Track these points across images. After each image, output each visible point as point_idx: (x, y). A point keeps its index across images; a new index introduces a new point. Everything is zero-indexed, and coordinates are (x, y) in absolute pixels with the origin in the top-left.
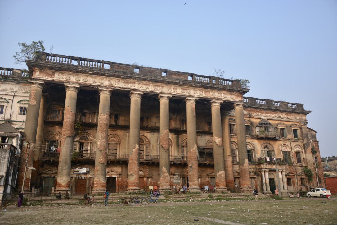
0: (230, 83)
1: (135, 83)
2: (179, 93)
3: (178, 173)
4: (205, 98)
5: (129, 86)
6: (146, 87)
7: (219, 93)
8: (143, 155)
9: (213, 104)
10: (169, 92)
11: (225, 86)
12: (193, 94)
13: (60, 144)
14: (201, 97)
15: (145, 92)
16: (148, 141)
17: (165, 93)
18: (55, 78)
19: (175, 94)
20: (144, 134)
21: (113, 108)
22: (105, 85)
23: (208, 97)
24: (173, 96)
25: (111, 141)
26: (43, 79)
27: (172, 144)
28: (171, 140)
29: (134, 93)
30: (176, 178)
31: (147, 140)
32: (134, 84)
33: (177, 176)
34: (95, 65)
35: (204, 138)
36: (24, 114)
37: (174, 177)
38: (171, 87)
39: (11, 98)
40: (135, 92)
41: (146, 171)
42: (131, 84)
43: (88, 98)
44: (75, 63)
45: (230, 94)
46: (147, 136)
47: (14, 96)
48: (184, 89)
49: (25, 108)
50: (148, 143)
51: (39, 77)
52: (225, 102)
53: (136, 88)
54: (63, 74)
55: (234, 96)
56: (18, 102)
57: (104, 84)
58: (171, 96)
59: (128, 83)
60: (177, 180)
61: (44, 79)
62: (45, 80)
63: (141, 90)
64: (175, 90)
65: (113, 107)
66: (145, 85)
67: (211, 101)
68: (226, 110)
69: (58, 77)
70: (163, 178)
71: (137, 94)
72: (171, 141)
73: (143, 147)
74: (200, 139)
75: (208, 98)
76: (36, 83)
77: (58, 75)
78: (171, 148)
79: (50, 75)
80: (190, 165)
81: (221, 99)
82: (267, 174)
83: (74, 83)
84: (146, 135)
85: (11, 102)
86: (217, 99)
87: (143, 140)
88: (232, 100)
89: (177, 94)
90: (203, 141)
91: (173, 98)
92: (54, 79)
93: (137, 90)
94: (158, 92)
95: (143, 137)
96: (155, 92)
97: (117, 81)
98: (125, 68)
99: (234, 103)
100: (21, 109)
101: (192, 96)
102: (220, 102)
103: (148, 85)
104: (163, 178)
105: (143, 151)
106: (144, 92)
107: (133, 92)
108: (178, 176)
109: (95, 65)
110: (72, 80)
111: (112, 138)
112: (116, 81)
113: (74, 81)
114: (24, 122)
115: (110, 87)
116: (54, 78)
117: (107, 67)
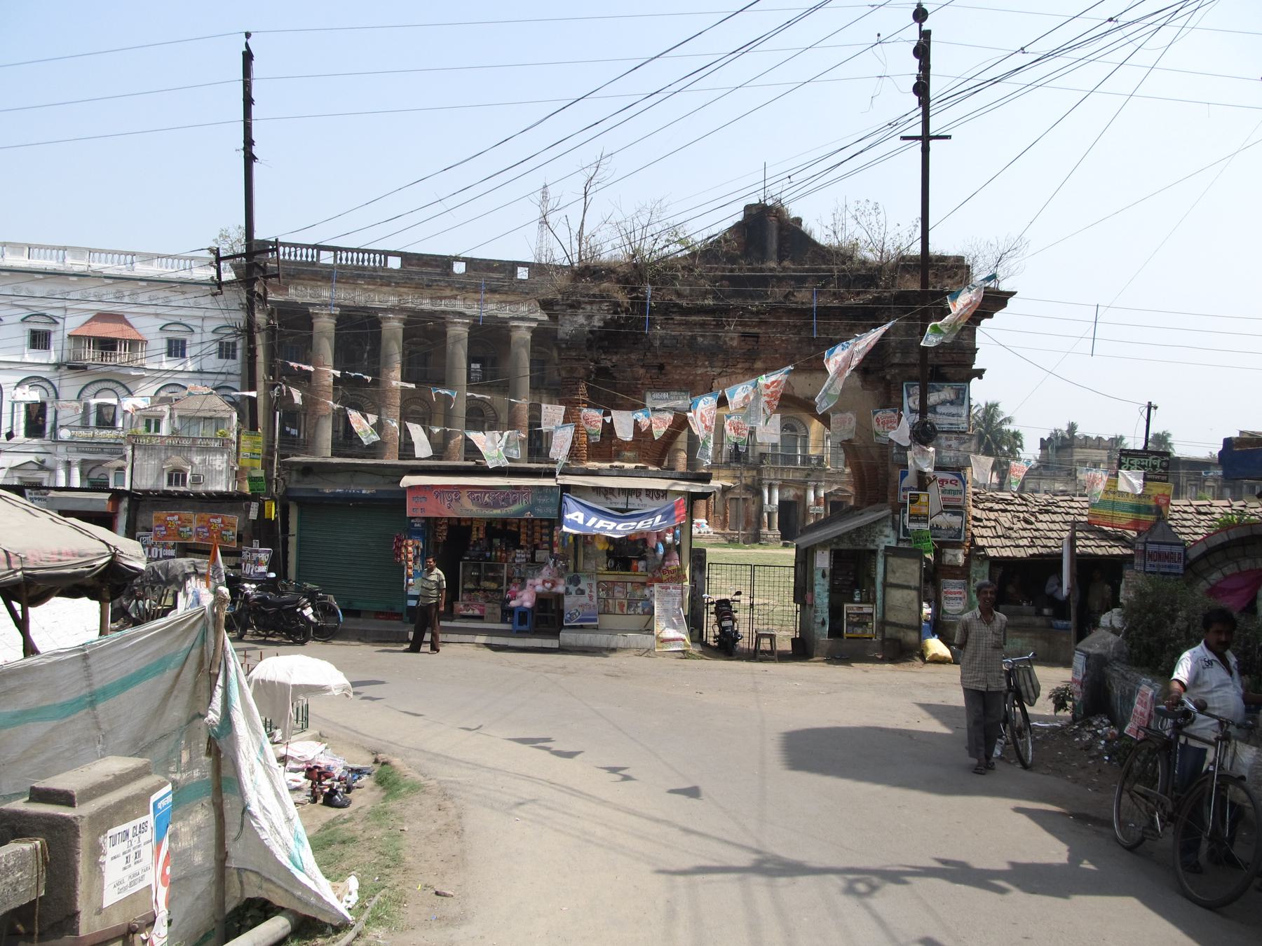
5: (442, 306)
10: (532, 316)
17: (522, 319)
32: (453, 302)
34: (369, 260)
39: (199, 322)
43: (358, 333)
44: (327, 258)
47: (203, 319)
53: (458, 309)
56: (213, 332)
58: (534, 325)
59: (441, 298)
63: (468, 312)
66: (478, 300)
69: (297, 294)
82: (776, 493)
85: (197, 330)
93: (461, 315)
109: (369, 260)
111: (413, 407)
115: (402, 310)
117: (395, 263)
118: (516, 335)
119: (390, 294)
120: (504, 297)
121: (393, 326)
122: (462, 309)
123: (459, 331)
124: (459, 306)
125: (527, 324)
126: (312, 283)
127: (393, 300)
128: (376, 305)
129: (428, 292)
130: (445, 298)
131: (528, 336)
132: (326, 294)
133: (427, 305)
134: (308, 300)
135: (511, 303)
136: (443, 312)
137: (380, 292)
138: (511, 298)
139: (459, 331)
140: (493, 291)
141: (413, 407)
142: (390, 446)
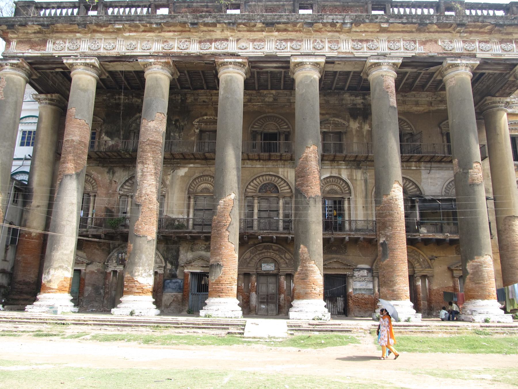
0: (500, 13)
1: (227, 40)
2: (346, 53)
3: (366, 264)
4: (425, 58)
5: (213, 48)
6: (257, 47)
7: (464, 42)
8: (278, 221)
9: (449, 71)
10: (317, 52)
11: (480, 19)
12: (387, 51)
13: (94, 204)
14: (410, 54)
15: (252, 60)
16: (287, 187)
18: (47, 50)
19: (334, 54)
20: (278, 173)
21: (205, 118)
22: (154, 52)
23: (433, 54)
24: (327, 62)
25: (201, 192)
26: (22, 54)
27: (350, 193)
28: (347, 183)
29: (223, 64)
30: (362, 276)
31: (285, 185)
32: (225, 43)
33: (365, 273)
35: (437, 176)
36: (28, 144)
37: (356, 274)
38: (323, 40)
40: (226, 60)
41: (282, 258)
42: (218, 43)
45: (502, 41)
46: (286, 176)
48: (361, 41)
49: (30, 132)
50: (288, 193)
51: (15, 51)
52: (485, 62)
54: (64, 40)
55: (514, 45)
57: (153, 50)
59: (211, 41)
60: (364, 283)
61: (25, 55)
62: (26, 58)
64: (334, 46)
65: (206, 115)
66: (254, 41)
67: (441, 63)
68: (494, 96)
70: (300, 274)
71: (230, 63)
72: (348, 186)
73: (278, 203)
74: (428, 178)
75: (432, 57)
76: (6, 65)
77: (54, 43)
78: (349, 203)
79: (38, 44)
80: (381, 241)
81: (474, 56)
83: (85, 56)
84: (284, 176)
86: (459, 56)
87: (276, 187)
88: (507, 57)
89: (341, 55)
90: (434, 183)
91: (331, 68)
92: (44, 52)
94: (289, 54)
95: (277, 179)
96: (279, 54)
97: (183, 40)
98: (205, 9)
99: (515, 65)
100: (23, 134)
101: (384, 55)
102: (472, 62)
103: (261, 40)
104: (300, 274)
105: (277, 211)
106: (250, 57)
107: (223, 60)
108: (366, 272)
110: (83, 51)
111: (204, 186)
112: (180, 42)
113: (87, 51)
114: (26, 159)
115: (166, 55)
116: (45, 50)
118: (299, 75)
119: (153, 41)
120: (284, 35)
121: (159, 79)
123: (233, 78)
124: (232, 47)
125: (313, 60)
126: (71, 35)
127: (157, 47)
128: (138, 52)
129: (196, 36)
130: (216, 40)
131: (316, 76)
132: (85, 46)
133: (194, 48)
134: (66, 52)
135: (292, 40)
136: (213, 55)
137: (143, 39)
138: (293, 35)
139: (233, 78)
140: (269, 25)
141: (204, 186)
142: (144, 209)
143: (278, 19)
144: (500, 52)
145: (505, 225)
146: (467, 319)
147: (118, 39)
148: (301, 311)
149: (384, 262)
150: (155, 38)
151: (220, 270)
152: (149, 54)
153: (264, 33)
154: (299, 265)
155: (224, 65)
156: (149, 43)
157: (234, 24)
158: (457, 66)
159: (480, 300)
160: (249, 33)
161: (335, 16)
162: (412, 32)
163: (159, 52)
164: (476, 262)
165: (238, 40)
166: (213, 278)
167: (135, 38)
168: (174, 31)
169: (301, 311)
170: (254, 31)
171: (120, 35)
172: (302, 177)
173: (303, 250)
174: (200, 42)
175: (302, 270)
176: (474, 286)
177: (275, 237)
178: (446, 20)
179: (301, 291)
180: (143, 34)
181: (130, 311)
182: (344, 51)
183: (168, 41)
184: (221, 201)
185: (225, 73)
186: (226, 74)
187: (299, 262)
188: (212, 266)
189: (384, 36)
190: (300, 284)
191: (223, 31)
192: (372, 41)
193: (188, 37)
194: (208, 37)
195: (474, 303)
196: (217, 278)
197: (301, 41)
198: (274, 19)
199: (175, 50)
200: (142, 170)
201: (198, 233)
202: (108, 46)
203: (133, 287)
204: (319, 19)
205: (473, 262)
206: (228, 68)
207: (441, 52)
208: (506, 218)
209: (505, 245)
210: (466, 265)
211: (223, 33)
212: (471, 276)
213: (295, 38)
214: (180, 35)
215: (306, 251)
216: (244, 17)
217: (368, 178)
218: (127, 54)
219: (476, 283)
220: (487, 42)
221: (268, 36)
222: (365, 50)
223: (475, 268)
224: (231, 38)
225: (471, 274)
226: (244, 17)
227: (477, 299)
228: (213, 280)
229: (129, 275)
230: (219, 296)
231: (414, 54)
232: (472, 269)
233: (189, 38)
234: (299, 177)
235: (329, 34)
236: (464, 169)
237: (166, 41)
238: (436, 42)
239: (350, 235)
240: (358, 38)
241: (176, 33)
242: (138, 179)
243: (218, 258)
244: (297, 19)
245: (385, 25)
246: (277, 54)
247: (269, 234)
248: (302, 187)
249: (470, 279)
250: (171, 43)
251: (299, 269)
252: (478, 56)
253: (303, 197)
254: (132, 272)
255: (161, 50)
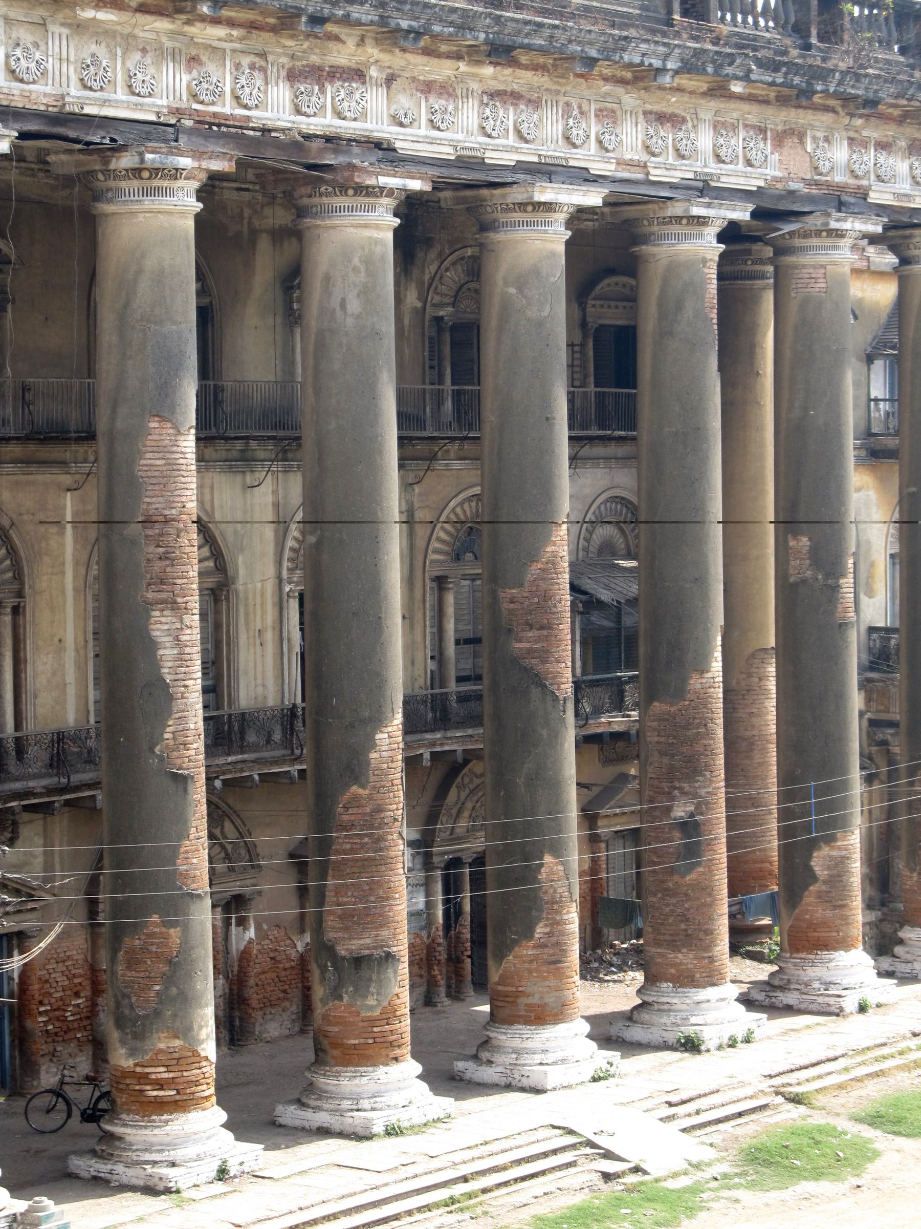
1: (358, 74)
12: (713, 168)
38: (585, 107)
58: (593, 198)
59: (322, 75)
66: (428, 88)
75: (792, 193)
94: (509, 159)
96: (492, 157)
97: (246, 61)
103: (445, 89)
107: (371, 181)
119: (162, 54)
122: (383, 129)
124: (370, 112)
128: (119, 105)
129: (284, 49)
133: (276, 107)
137: (129, 42)
143: (527, 35)
144: (905, 187)
145: (750, 675)
146: (813, 1007)
147: (52, 28)
148: (564, 1061)
149: (688, 878)
150: (168, 44)
151: (395, 972)
152: (153, 118)
153: (463, 67)
154: (539, 919)
155: (368, 195)
156: (148, 60)
157: (418, 34)
158: (839, 234)
159: (842, 952)
160: (425, 59)
161: (652, 46)
162: (766, 102)
163: (178, 112)
164: (839, 848)
165: (390, 80)
166: (371, 1002)
167: (106, 32)
168: (231, 23)
169: (564, 1061)
170: (439, 56)
171: (60, 16)
172: (542, 628)
173: (551, 872)
174: (292, 76)
175: (549, 934)
176: (829, 913)
177: (256, 777)
178: (853, 87)
179: (550, 999)
180: (141, 18)
181: (215, 1165)
182: (628, 157)
183: (204, 59)
184: (378, 736)
185: (366, 226)
186: (367, 233)
187: (541, 911)
188: (358, 961)
189: (709, 109)
190: (545, 979)
191: (362, 41)
192: (684, 120)
193: (259, 48)
194: (315, 59)
195: (830, 961)
196: (385, 1003)
197: (535, 104)
198: (519, 32)
199: (227, 108)
200: (177, 639)
201: (50, 791)
202: (24, 63)
203: (197, 1084)
204: (614, 51)
205: (833, 848)
206: (373, 208)
207: (808, 176)
208: (753, 656)
209: (744, 739)
210: (810, 857)
211: (360, 50)
212: (824, 888)
213: (523, 90)
214: (241, 39)
215: (562, 873)
216: (454, 17)
217: (416, 505)
218: (88, 110)
219: (836, 907)
220: (883, 146)
221: (467, 74)
222: (671, 161)
223: (836, 866)
224: (373, 72)
225: (825, 882)
226: (454, 17)
227: (835, 949)
228: (371, 1008)
229: (177, 1043)
230: (396, 1059)
231: (761, 183)
232: (829, 868)
233: (263, 55)
234: (531, 627)
235: (607, 88)
236: (827, 575)
237: (193, 60)
238: (801, 137)
239: (433, 744)
240: (656, 108)
241: (235, 33)
242: (166, 673)
243: (385, 933)
244: (570, 41)
245: (737, 88)
246: (488, 154)
247: (242, 770)
248: (545, 662)
249: (819, 895)
250: (211, 67)
251: (540, 930)
252: (874, 197)
253: (549, 698)
254: (190, 1029)
255: (184, 102)
